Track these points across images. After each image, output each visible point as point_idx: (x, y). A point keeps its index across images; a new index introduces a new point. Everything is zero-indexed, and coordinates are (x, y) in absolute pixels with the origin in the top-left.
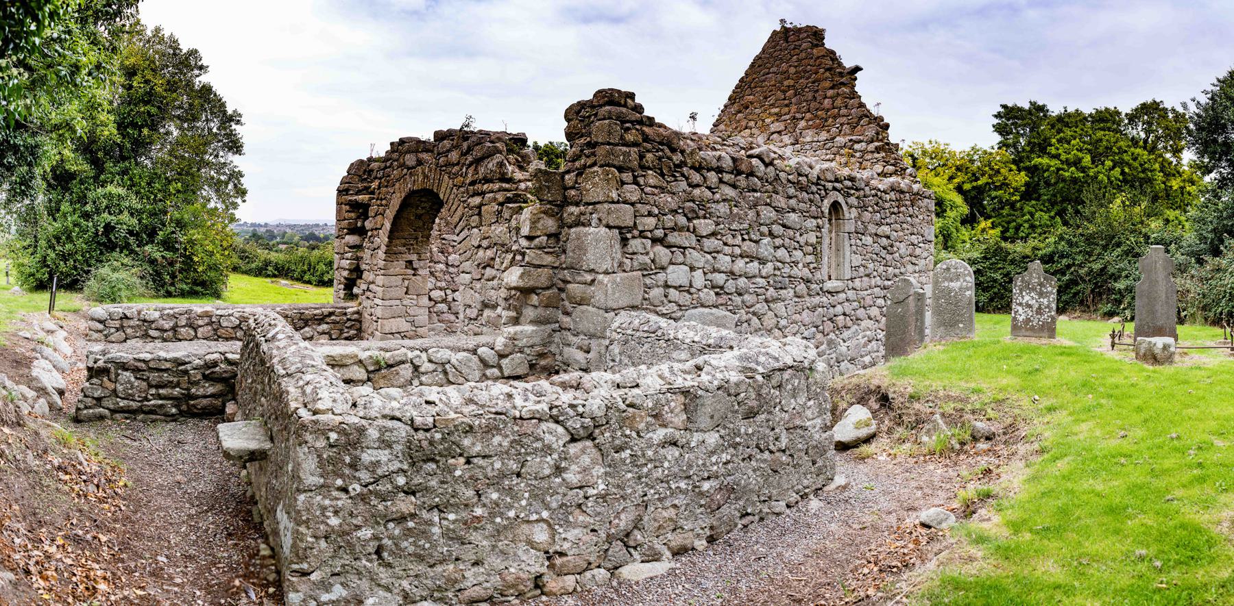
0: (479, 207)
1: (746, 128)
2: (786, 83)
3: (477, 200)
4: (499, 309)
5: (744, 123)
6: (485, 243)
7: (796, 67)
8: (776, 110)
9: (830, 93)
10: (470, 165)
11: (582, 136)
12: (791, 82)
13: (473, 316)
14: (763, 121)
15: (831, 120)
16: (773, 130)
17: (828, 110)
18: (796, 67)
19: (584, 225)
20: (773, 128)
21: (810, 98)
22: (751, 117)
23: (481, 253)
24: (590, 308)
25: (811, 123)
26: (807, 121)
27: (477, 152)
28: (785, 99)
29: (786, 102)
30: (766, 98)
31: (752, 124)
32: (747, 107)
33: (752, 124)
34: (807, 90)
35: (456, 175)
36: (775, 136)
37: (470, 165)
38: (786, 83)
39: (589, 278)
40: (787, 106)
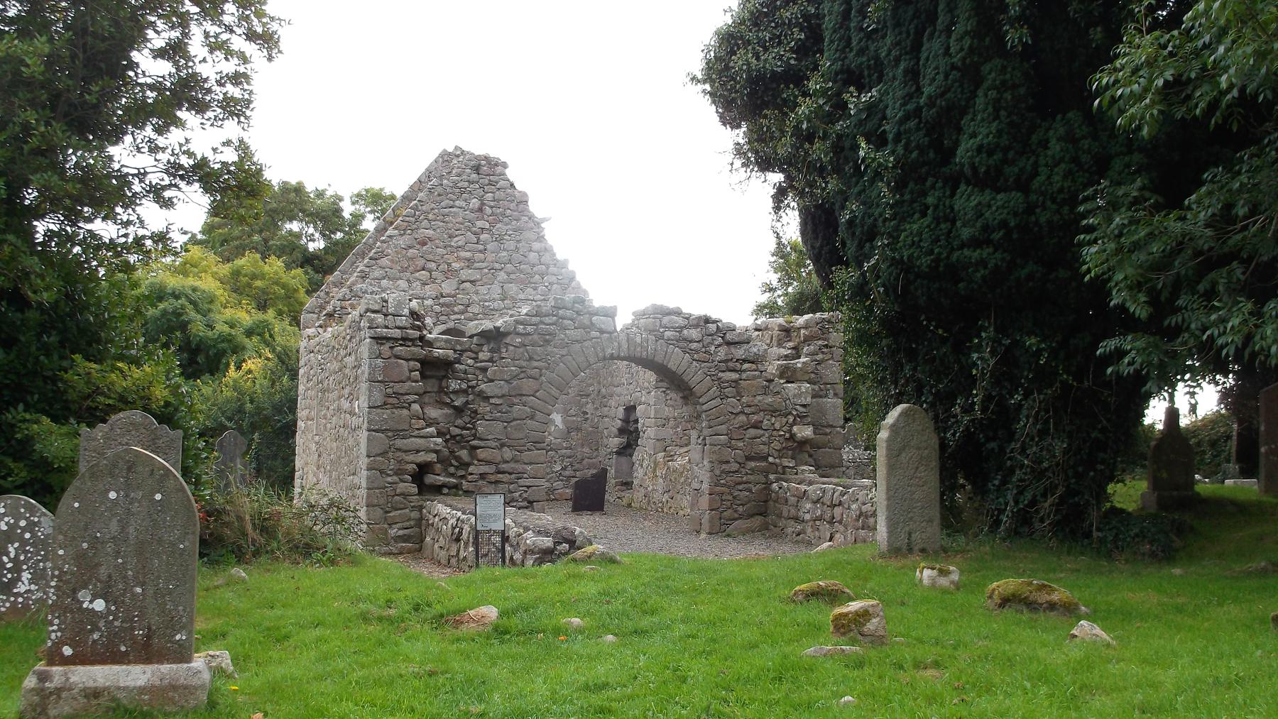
0: (736, 381)
1: (423, 270)
2: (480, 224)
3: (735, 376)
4: (771, 459)
5: (421, 262)
6: (747, 410)
7: (492, 207)
8: (468, 255)
9: (536, 246)
10: (719, 346)
11: (819, 339)
12: (487, 226)
13: (733, 469)
14: (449, 265)
15: (537, 276)
16: (464, 278)
17: (534, 266)
18: (492, 207)
19: (821, 397)
20: (465, 274)
21: (512, 248)
22: (431, 257)
23: (742, 418)
24: (827, 449)
25: (513, 276)
26: (508, 274)
27: (729, 337)
28: (477, 243)
29: (481, 247)
30: (451, 237)
31: (433, 265)
32: (424, 244)
33: (433, 265)
34: (507, 237)
35: (697, 352)
36: (467, 285)
37: (719, 346)
38: (480, 224)
39: (828, 430)
40: (481, 252)
